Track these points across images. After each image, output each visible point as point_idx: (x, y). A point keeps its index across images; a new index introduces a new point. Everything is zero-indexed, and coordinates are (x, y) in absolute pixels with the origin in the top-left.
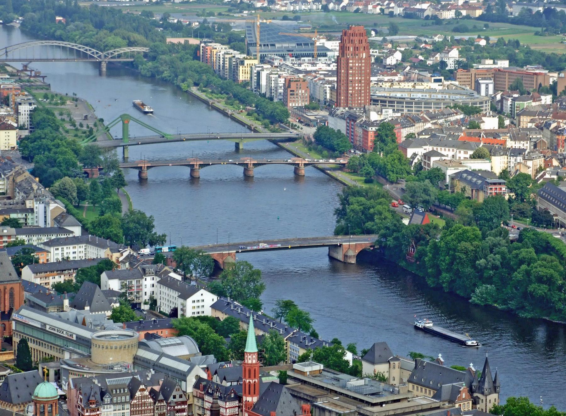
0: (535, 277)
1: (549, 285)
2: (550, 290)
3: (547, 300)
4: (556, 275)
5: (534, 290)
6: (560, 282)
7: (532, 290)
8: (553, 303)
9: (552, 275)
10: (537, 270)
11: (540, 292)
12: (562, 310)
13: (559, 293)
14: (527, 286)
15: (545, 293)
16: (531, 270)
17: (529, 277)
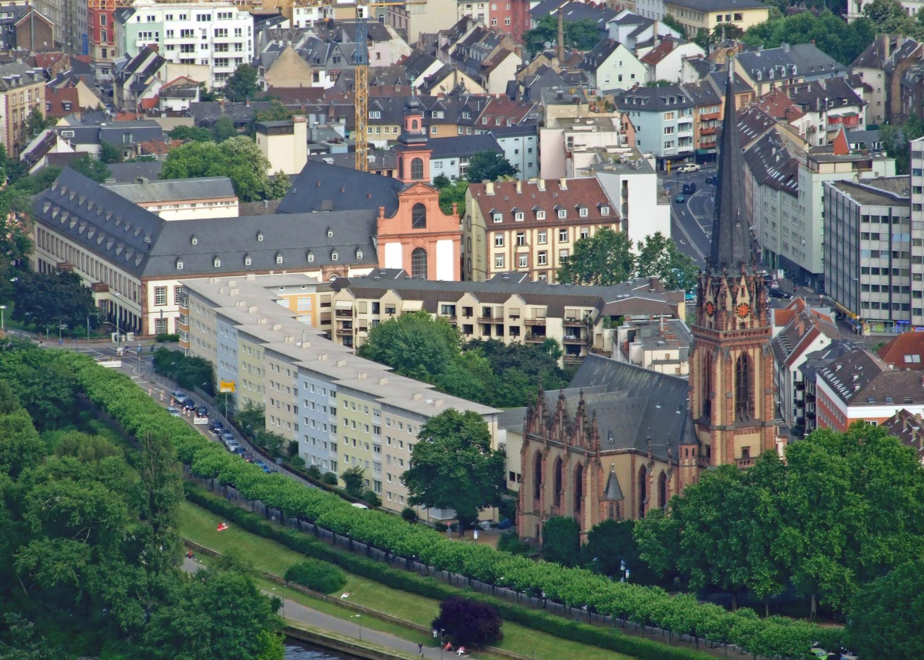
0: (40, 514)
1: (92, 542)
2: (95, 560)
3: (87, 596)
4: (117, 504)
5: (39, 563)
6: (131, 528)
7: (33, 562)
8: (109, 606)
9: (101, 508)
10: (47, 489)
11: (60, 566)
12: (142, 630)
13: (130, 569)
14: (14, 548)
15: (78, 570)
16: (23, 492)
17: (17, 517)
